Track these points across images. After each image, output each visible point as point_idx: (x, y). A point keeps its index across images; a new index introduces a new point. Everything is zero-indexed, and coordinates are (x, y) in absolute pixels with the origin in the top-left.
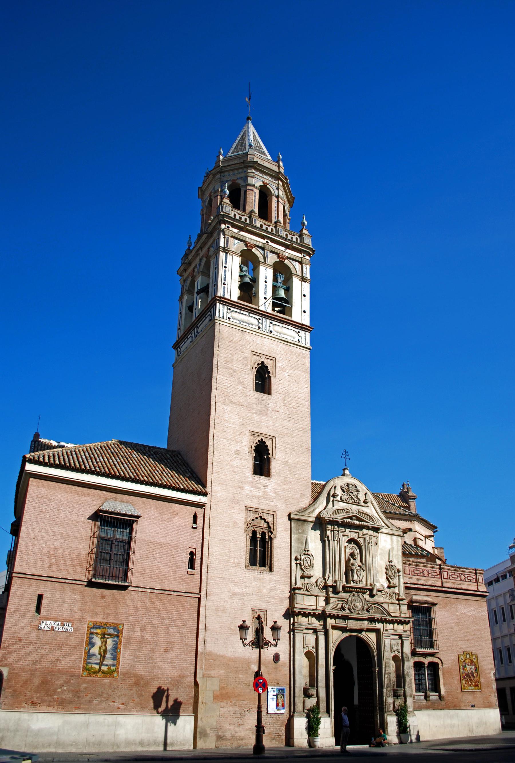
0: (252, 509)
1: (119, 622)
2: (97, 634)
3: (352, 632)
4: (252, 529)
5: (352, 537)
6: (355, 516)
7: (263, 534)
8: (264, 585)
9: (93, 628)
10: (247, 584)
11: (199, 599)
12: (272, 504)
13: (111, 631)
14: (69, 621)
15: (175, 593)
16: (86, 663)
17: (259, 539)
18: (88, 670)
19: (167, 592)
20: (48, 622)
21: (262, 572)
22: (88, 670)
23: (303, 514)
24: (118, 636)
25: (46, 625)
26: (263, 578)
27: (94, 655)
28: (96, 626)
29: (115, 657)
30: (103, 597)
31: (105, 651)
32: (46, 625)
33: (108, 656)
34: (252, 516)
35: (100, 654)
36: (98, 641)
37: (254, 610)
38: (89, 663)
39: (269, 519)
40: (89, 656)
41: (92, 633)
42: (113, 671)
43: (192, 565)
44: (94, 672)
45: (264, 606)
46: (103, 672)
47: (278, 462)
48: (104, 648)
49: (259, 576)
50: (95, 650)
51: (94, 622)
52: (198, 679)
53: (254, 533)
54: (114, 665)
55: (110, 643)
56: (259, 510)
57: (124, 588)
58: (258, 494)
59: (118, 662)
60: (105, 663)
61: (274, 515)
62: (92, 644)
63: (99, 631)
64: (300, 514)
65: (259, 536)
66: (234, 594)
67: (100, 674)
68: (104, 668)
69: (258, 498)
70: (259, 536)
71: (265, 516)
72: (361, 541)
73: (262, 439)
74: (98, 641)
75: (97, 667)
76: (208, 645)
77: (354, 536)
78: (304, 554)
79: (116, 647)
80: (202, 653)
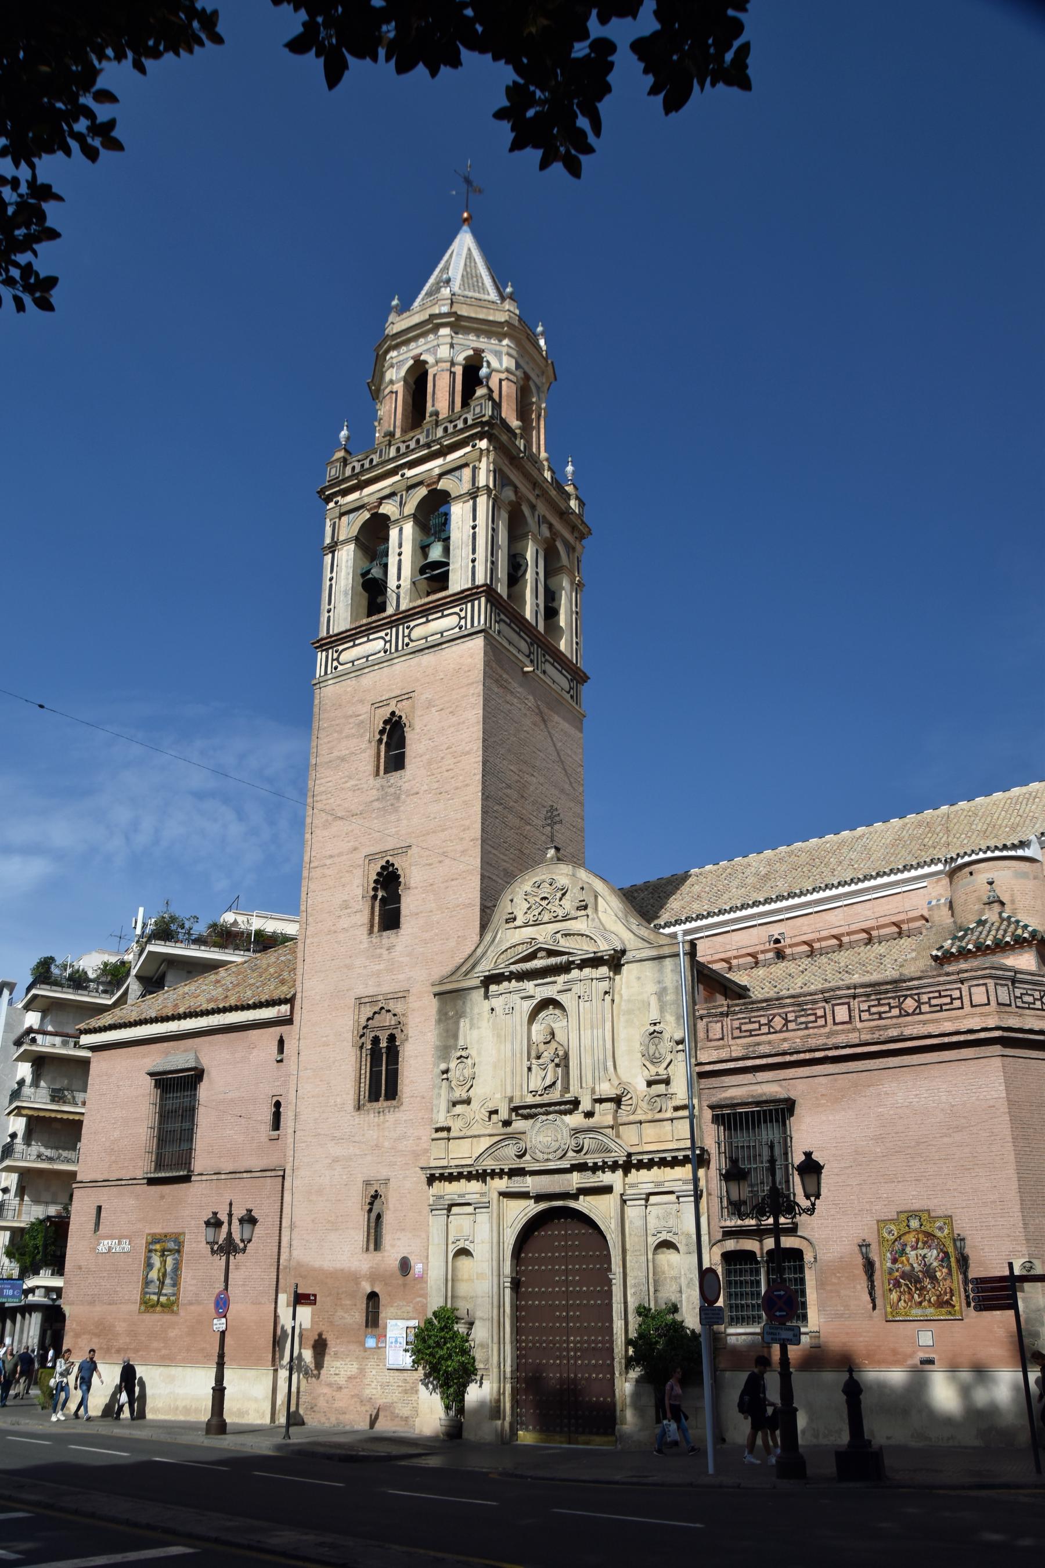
0: (367, 1000)
1: (180, 1230)
2: (156, 1251)
3: (551, 1201)
4: (373, 1034)
7: (392, 1038)
8: (386, 1134)
9: (152, 1243)
10: (356, 1139)
11: (283, 1177)
12: (401, 977)
13: (171, 1245)
14: (126, 1237)
15: (249, 1175)
16: (144, 1293)
17: (384, 1050)
18: (145, 1303)
19: (238, 1176)
20: (106, 1242)
22: (145, 1303)
24: (178, 1251)
25: (104, 1246)
27: (152, 1281)
28: (155, 1239)
29: (176, 1284)
30: (162, 1197)
31: (164, 1275)
32: (104, 1246)
33: (168, 1281)
34: (368, 1011)
35: (159, 1279)
36: (156, 1260)
38: (147, 1293)
40: (147, 1283)
41: (150, 1251)
42: (173, 1303)
43: (276, 1124)
44: (153, 1306)
45: (384, 1172)
46: (162, 1306)
47: (416, 891)
48: (163, 1270)
49: (376, 1119)
50: (154, 1275)
51: (153, 1235)
52: (279, 1311)
53: (376, 1040)
54: (174, 1295)
55: (170, 1260)
56: (380, 998)
57: (186, 1179)
58: (377, 967)
59: (179, 1290)
60: (164, 1291)
62: (149, 1266)
63: (158, 1247)
65: (383, 1044)
66: (336, 1160)
67: (159, 1309)
68: (163, 1299)
69: (378, 974)
70: (383, 1044)
71: (391, 1005)
73: (388, 862)
74: (156, 1260)
75: (155, 1298)
76: (295, 1253)
79: (177, 1268)
80: (286, 1268)
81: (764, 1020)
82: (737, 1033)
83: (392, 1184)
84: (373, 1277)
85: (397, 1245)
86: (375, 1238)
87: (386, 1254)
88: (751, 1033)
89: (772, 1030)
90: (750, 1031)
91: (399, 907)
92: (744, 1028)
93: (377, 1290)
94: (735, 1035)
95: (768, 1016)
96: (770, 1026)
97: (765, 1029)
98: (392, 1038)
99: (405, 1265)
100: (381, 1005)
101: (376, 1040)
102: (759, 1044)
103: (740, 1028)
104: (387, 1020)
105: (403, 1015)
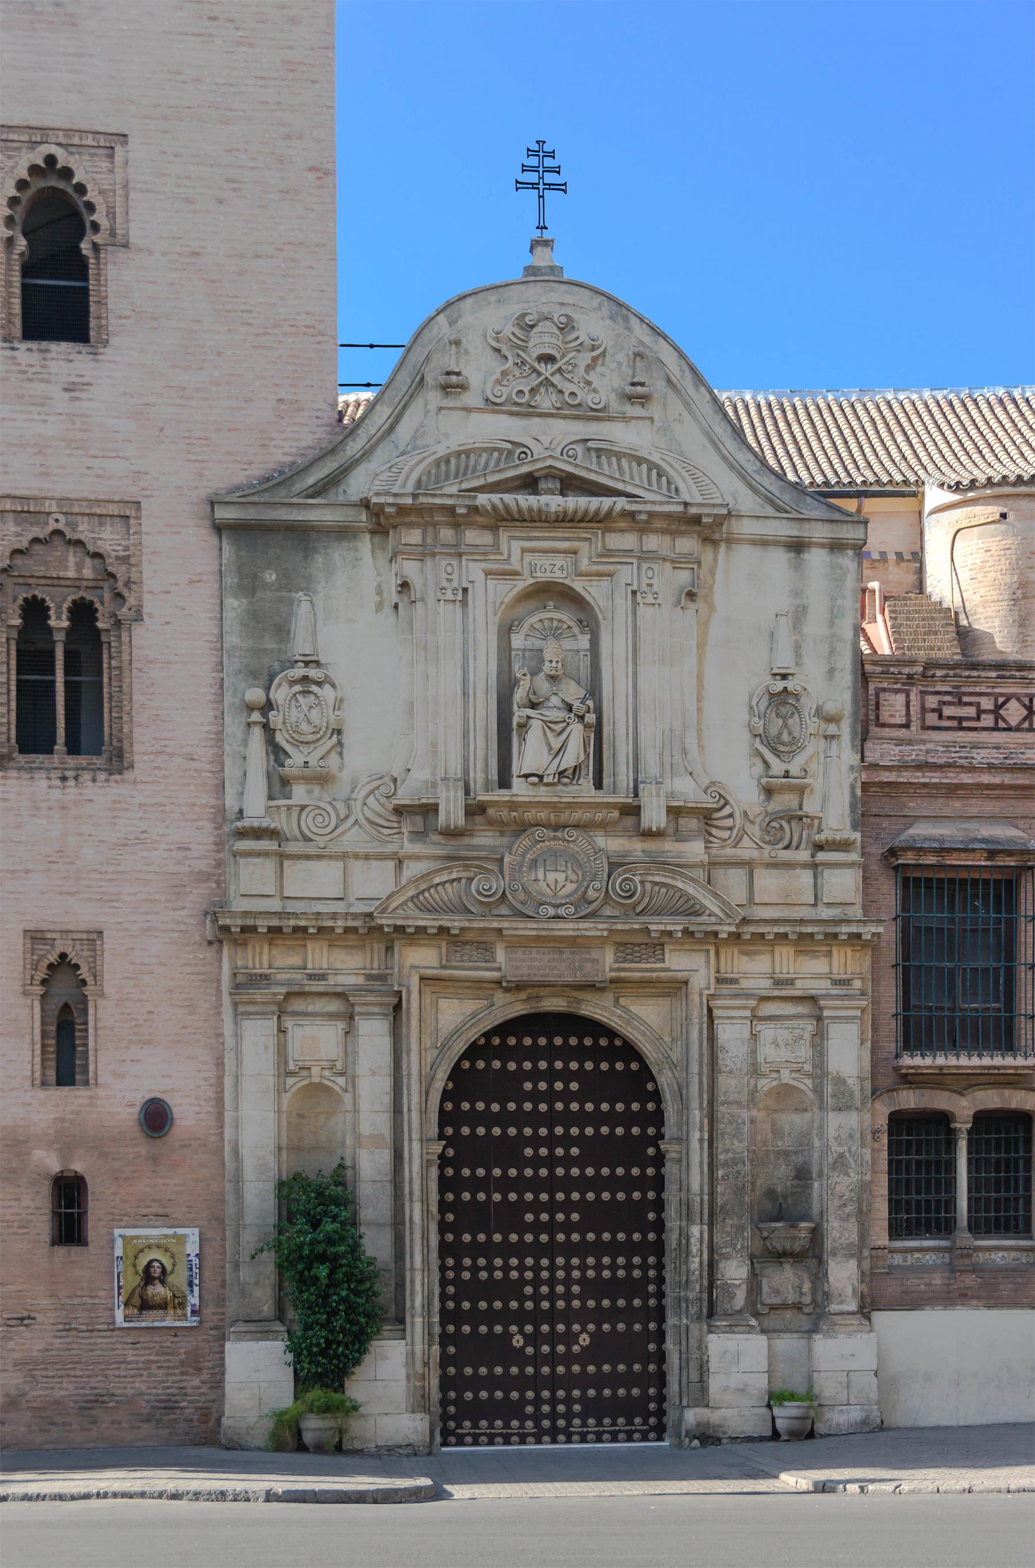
4: (24, 594)
5: (542, 577)
6: (551, 473)
7: (83, 613)
17: (59, 637)
21: (69, 774)
23: (280, 496)
26: (76, 803)
37: (35, 937)
39: (109, 539)
45: (83, 915)
49: (57, 794)
53: (35, 610)
61: (127, 515)
64: (266, 497)
65: (59, 622)
70: (59, 622)
71: (84, 531)
72: (594, 592)
73: (51, 160)
77: (554, 569)
78: (293, 683)
81: (987, 704)
82: (932, 719)
83: (110, 943)
84: (66, 1141)
85: (124, 1074)
86: (65, 1053)
87: (101, 1092)
88: (960, 724)
89: (1002, 724)
90: (960, 719)
91: (85, 291)
92: (947, 711)
93: (78, 1166)
94: (928, 723)
95: (996, 696)
96: (998, 717)
97: (987, 721)
98: (83, 613)
99: (156, 1118)
100: (52, 526)
101: (35, 610)
102: (975, 746)
103: (939, 712)
104: (72, 566)
105: (124, 560)
